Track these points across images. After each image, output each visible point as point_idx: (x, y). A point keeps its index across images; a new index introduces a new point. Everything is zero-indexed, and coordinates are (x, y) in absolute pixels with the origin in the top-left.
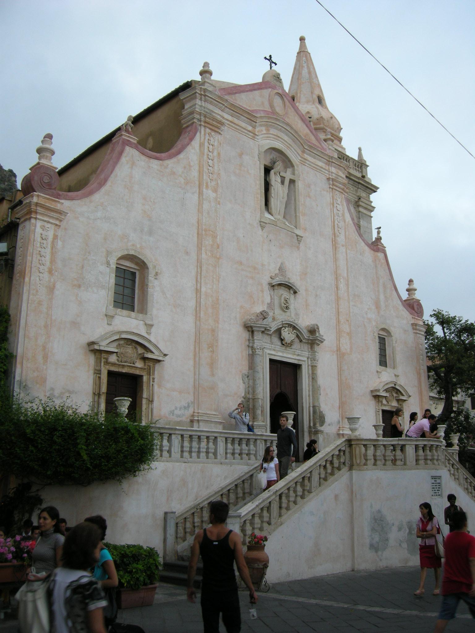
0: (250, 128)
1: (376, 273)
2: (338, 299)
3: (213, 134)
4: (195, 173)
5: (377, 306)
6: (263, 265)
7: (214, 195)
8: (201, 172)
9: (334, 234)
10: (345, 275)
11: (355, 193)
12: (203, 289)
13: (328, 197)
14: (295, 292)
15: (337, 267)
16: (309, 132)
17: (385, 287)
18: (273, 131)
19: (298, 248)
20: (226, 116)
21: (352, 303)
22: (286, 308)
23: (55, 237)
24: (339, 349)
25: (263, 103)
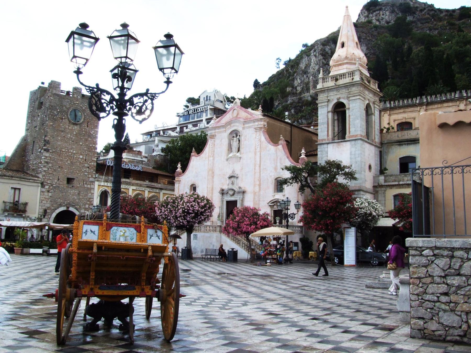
0: (224, 129)
1: (276, 155)
2: (255, 173)
3: (212, 140)
4: (207, 154)
5: (276, 169)
6: (227, 172)
7: (212, 158)
8: (209, 153)
9: (255, 149)
10: (259, 163)
11: (347, 91)
12: (209, 187)
13: (254, 136)
14: (237, 178)
15: (255, 161)
16: (247, 114)
17: (281, 159)
18: (232, 125)
19: (240, 161)
20: (217, 131)
21: (261, 172)
22: (233, 184)
23: (179, 186)
24: (254, 191)
25: (230, 117)
